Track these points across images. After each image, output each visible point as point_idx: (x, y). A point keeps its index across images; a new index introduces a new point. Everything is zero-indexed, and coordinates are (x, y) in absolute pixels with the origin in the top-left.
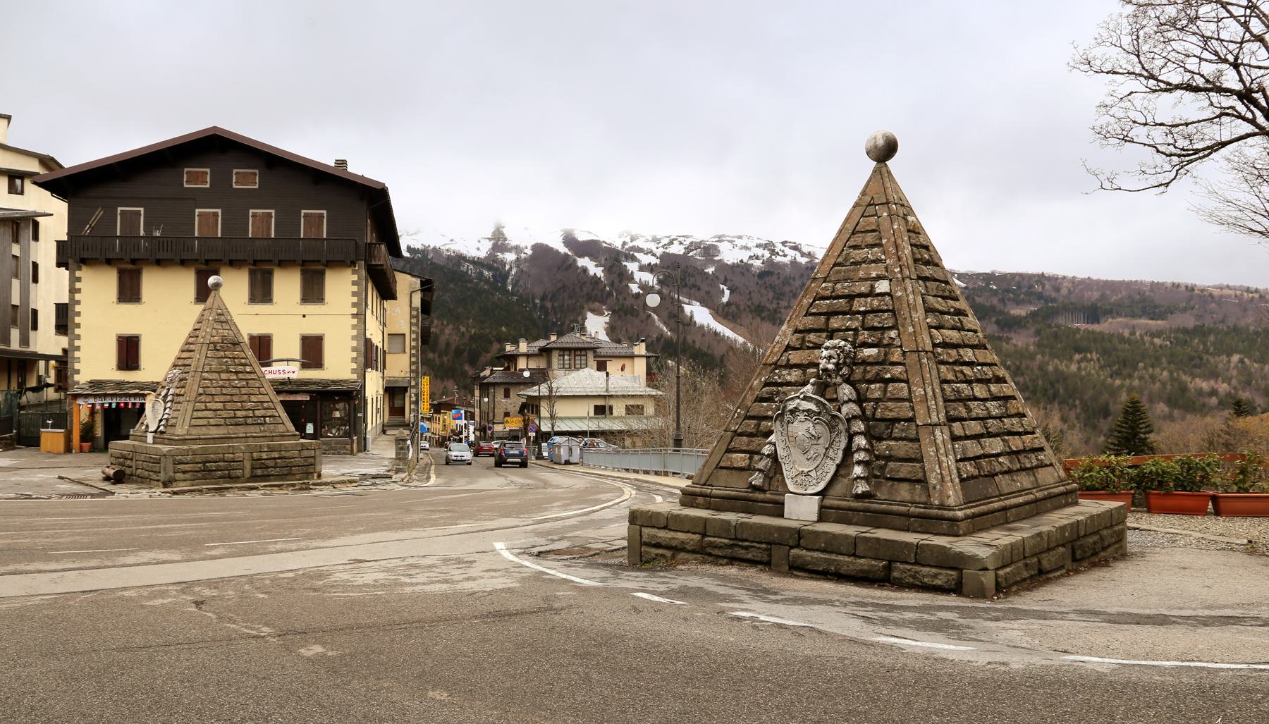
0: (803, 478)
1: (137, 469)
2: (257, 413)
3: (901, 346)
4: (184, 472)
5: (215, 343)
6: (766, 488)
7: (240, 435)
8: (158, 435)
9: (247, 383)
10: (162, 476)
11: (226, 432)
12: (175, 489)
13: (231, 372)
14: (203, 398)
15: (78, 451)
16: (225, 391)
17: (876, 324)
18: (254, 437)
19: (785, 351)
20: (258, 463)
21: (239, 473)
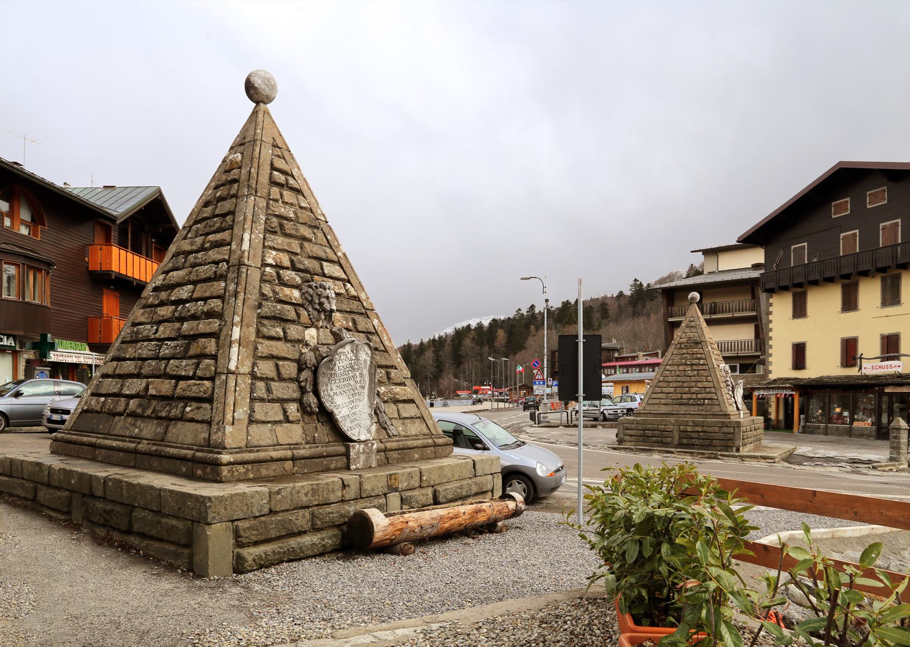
2: (699, 396)
4: (631, 436)
5: (681, 344)
11: (671, 409)
13: (688, 364)
14: (661, 384)
18: (691, 414)
20: (684, 434)
21: (669, 440)
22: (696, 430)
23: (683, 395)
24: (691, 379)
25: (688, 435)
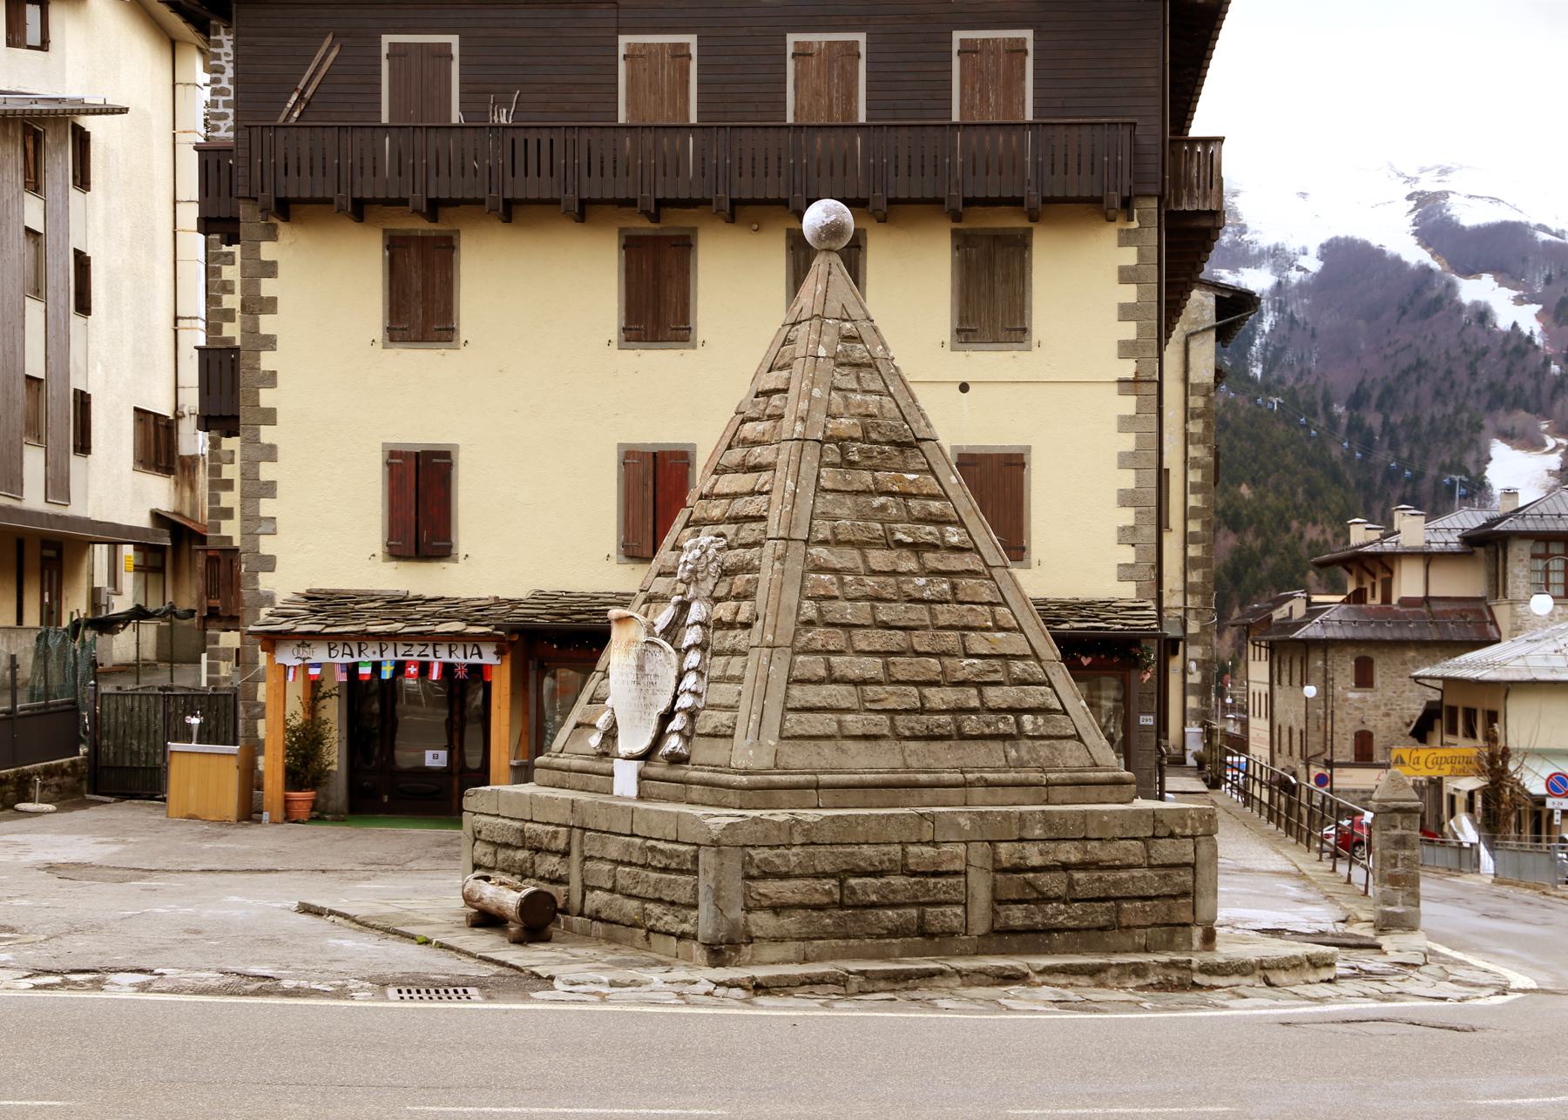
1: (586, 888)
2: (995, 696)
4: (778, 909)
5: (841, 441)
7: (946, 777)
8: (658, 769)
9: (954, 587)
10: (704, 921)
11: (897, 762)
12: (761, 973)
13: (900, 544)
14: (818, 636)
15: (280, 815)
16: (885, 613)
18: (989, 784)
22: (1063, 858)
23: (927, 691)
24: (933, 615)
25: (1029, 884)
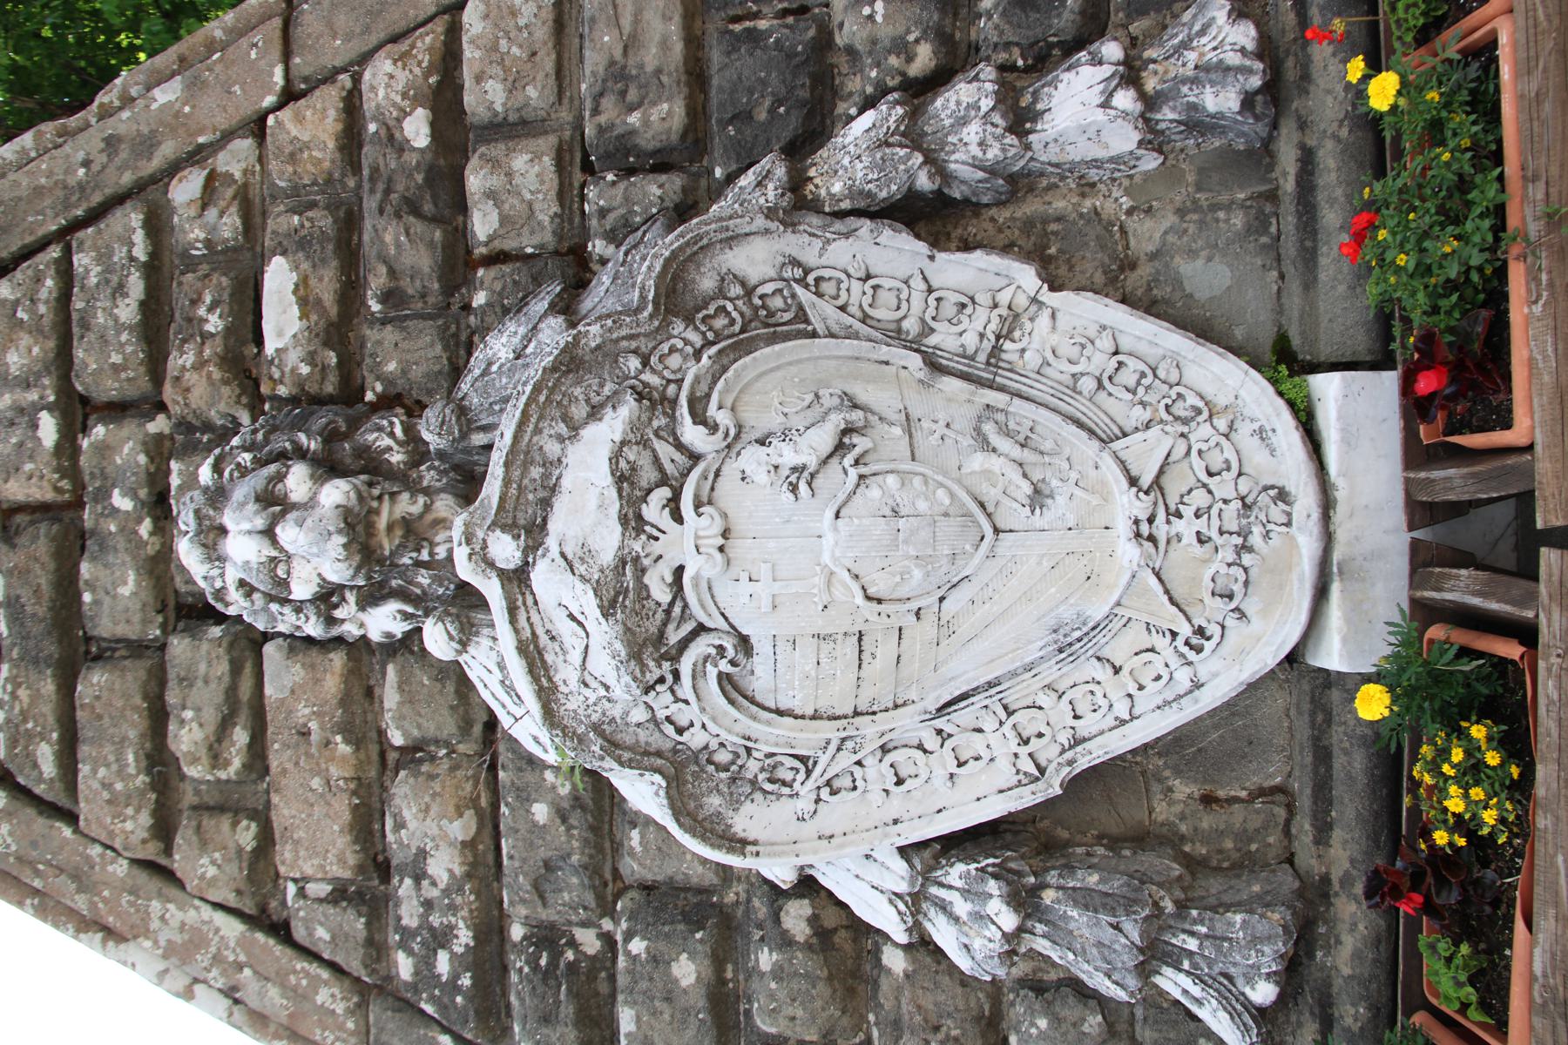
0: (1186, 527)
3: (257, 127)
6: (1287, 882)
17: (128, 311)
19: (281, 931)
